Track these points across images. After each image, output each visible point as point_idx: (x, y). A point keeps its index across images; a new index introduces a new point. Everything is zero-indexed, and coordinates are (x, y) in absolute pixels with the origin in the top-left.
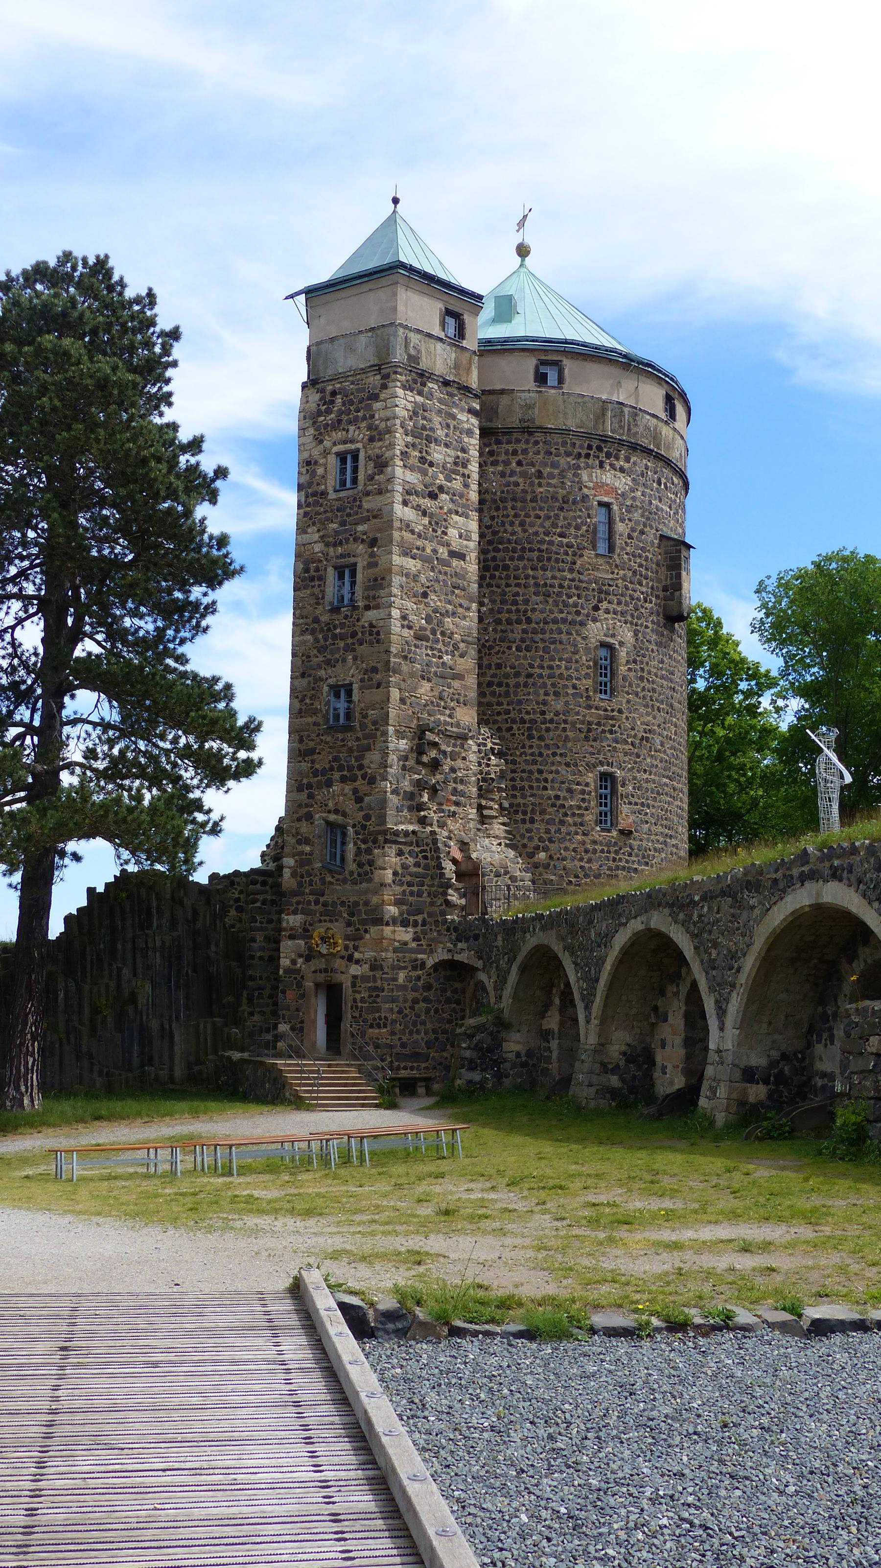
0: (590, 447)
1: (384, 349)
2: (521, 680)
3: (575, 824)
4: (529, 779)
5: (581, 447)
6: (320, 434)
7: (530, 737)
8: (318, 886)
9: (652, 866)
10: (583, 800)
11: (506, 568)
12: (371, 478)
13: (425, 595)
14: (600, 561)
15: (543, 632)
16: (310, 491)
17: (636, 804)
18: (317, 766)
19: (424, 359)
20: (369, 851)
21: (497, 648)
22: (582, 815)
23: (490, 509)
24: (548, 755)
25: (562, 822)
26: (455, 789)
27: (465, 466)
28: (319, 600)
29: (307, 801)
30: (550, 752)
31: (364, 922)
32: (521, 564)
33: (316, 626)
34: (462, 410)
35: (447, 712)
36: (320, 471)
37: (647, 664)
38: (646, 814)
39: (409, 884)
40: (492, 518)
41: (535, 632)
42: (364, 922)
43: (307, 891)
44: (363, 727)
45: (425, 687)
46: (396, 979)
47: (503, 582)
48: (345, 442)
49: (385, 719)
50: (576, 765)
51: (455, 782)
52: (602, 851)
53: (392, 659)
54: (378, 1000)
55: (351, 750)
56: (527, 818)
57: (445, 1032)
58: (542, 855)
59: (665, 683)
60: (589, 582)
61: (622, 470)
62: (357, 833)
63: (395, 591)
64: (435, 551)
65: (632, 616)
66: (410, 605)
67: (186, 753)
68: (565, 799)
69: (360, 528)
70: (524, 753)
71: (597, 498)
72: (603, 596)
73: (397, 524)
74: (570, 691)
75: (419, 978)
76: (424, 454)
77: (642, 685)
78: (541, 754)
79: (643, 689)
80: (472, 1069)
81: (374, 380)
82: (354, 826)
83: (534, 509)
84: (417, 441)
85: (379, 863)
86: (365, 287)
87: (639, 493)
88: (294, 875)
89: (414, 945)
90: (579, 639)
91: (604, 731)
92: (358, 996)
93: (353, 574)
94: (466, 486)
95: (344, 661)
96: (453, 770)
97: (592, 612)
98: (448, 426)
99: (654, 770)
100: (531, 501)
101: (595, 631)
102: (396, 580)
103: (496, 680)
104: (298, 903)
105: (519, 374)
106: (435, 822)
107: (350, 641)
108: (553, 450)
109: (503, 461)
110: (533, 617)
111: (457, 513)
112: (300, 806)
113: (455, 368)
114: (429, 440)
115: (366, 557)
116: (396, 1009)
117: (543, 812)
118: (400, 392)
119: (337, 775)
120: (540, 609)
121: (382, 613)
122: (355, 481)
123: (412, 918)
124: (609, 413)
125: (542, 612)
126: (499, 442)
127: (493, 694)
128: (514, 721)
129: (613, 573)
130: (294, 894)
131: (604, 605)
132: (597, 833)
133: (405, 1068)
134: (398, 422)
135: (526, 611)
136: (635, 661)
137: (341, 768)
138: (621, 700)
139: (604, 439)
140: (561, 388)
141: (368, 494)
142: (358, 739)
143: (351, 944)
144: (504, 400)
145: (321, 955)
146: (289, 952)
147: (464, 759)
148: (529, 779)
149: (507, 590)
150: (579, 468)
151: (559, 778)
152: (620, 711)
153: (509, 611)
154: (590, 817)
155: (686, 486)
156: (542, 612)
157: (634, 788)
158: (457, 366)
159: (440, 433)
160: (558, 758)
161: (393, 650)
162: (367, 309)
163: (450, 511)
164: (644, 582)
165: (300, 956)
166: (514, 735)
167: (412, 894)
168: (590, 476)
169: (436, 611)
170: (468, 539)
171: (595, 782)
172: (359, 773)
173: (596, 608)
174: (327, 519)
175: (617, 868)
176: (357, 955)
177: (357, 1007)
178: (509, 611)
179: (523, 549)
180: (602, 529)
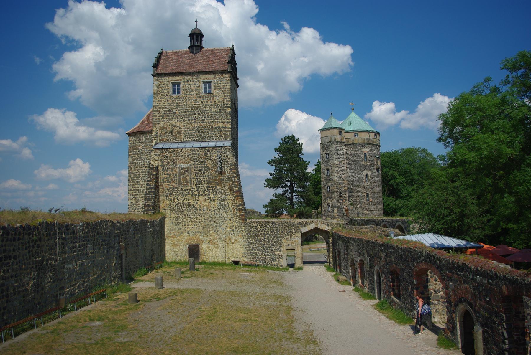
1: (331, 139)
139: (365, 144)
154: (365, 200)
162: (328, 133)
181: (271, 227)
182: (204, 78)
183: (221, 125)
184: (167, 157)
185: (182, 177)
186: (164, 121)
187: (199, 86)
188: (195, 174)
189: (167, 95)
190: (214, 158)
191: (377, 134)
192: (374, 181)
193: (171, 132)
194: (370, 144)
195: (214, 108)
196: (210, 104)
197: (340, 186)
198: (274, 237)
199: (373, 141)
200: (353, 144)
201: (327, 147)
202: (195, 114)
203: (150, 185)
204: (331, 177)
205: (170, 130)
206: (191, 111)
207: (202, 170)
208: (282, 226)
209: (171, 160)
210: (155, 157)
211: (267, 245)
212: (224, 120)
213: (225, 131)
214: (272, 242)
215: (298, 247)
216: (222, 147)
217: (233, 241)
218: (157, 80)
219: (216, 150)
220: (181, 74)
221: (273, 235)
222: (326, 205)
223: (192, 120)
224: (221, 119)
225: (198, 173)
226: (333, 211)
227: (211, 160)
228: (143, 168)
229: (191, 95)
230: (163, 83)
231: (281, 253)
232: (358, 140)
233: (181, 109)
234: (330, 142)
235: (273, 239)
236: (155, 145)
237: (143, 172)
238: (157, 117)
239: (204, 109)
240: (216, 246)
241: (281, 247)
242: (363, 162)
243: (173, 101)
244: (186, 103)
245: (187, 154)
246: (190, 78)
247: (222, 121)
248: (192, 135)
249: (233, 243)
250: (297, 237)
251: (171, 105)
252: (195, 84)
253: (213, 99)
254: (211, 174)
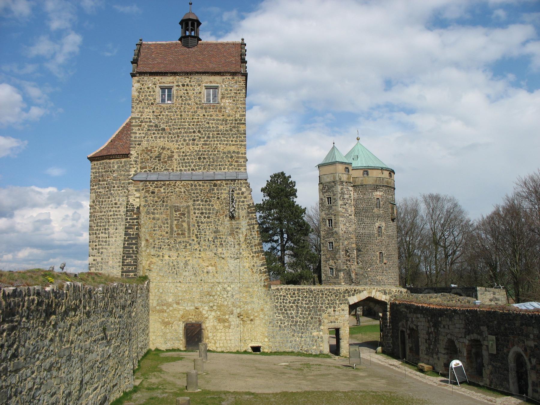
1: (334, 178)
81: (333, 184)
154: (378, 261)
159: (346, 192)
181: (306, 297)
182: (207, 80)
183: (233, 148)
184: (153, 193)
185: (175, 222)
186: (148, 141)
187: (200, 93)
188: (195, 218)
189: (152, 104)
190: (224, 196)
191: (392, 172)
192: (389, 236)
193: (159, 157)
194: (383, 186)
195: (222, 125)
196: (215, 118)
197: (346, 243)
198: (311, 311)
199: (387, 182)
200: (362, 185)
201: (329, 189)
202: (194, 132)
203: (130, 234)
204: (335, 229)
205: (157, 154)
206: (189, 128)
207: (206, 213)
208: (322, 294)
209: (159, 198)
210: (135, 193)
211: (300, 322)
212: (236, 141)
213: (238, 158)
214: (307, 318)
215: (344, 324)
216: (235, 180)
217: (252, 317)
218: (138, 82)
219: (227, 184)
220: (174, 74)
221: (309, 307)
222: (328, 268)
223: (190, 140)
224: (232, 141)
225: (200, 217)
226: (337, 277)
227: (218, 198)
228: (114, 209)
229: (189, 104)
230: (146, 87)
231: (321, 333)
232: (369, 180)
233: (173, 125)
234: (334, 182)
235: (309, 314)
236: (134, 175)
237: (114, 215)
238: (138, 135)
239: (207, 125)
240: (226, 324)
241: (320, 325)
242: (376, 210)
243: (161, 112)
244: (181, 115)
245: (183, 190)
246: (188, 80)
247: (234, 143)
248: (189, 163)
249: (252, 320)
250: (343, 310)
251: (158, 118)
252: (194, 90)
253: (220, 111)
254: (219, 220)
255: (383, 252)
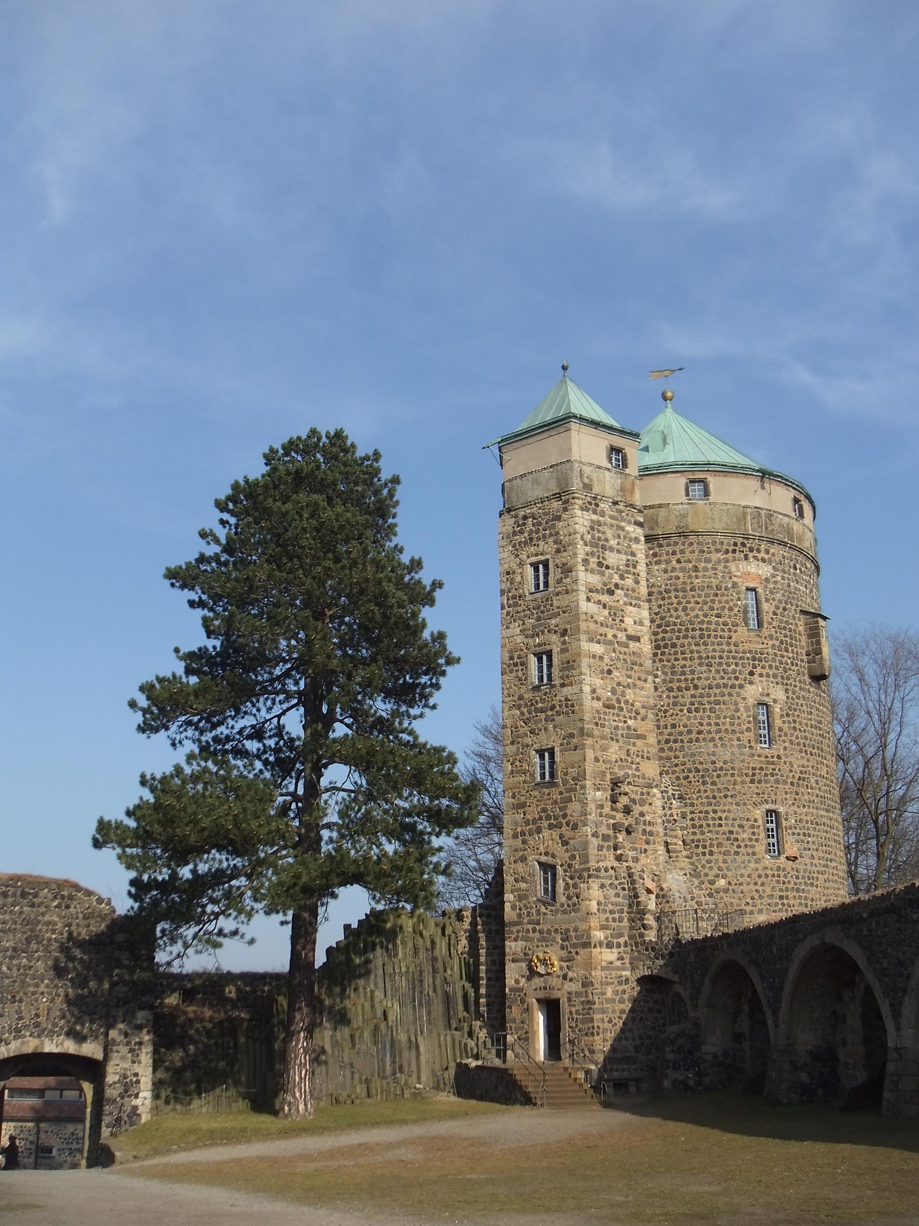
0: (735, 544)
2: (694, 736)
3: (748, 854)
4: (706, 818)
5: (729, 544)
6: (517, 550)
7: (704, 783)
8: (534, 917)
9: (817, 886)
10: (754, 833)
11: (674, 645)
12: (559, 581)
13: (609, 672)
14: (752, 634)
15: (709, 696)
16: (510, 595)
17: (799, 834)
18: (528, 817)
19: (596, 485)
20: (575, 886)
21: (672, 711)
22: (754, 846)
23: (657, 599)
24: (720, 797)
25: (737, 853)
26: (644, 830)
27: (635, 567)
28: (523, 680)
29: (522, 846)
30: (722, 795)
31: (575, 946)
32: (686, 641)
33: (521, 702)
34: (629, 523)
35: (634, 766)
36: (518, 579)
37: (798, 716)
38: (808, 843)
39: (611, 912)
40: (660, 606)
41: (702, 696)
42: (575, 946)
43: (525, 921)
44: (565, 782)
45: (614, 747)
46: (604, 994)
47: (673, 657)
48: (537, 555)
49: (582, 775)
50: (745, 804)
51: (645, 824)
52: (773, 875)
53: (586, 726)
54: (591, 1012)
55: (556, 802)
56: (707, 851)
57: (650, 1037)
58: (722, 882)
59: (815, 731)
60: (744, 652)
61: (763, 560)
62: (565, 871)
63: (584, 670)
64: (615, 636)
65: (782, 677)
66: (598, 682)
67: (421, 811)
68: (738, 833)
69: (553, 621)
70: (700, 796)
71: (745, 584)
72: (757, 662)
73: (583, 617)
74: (736, 743)
75: (624, 992)
76: (601, 560)
77: (796, 734)
78: (714, 797)
79: (797, 738)
80: (675, 1069)
81: (556, 505)
82: (562, 865)
83: (693, 596)
84: (595, 550)
85: (584, 895)
86: (546, 435)
87: (779, 578)
88: (513, 908)
89: (618, 963)
90: (739, 699)
91: (766, 775)
92: (573, 1009)
93: (550, 659)
94: (637, 582)
95: (546, 729)
96: (642, 814)
97: (748, 677)
98: (619, 536)
99: (811, 805)
100: (691, 590)
101: (752, 692)
102: (585, 662)
103: (672, 738)
104: (518, 932)
105: (672, 491)
106: (630, 859)
107: (550, 713)
108: (705, 549)
109: (665, 561)
110: (699, 684)
111: (631, 604)
112: (516, 850)
113: (621, 491)
114: (604, 547)
115: (560, 644)
116: (606, 1020)
117: (719, 845)
118: (578, 512)
119: (545, 824)
120: (705, 676)
121: (575, 689)
122: (546, 584)
123: (615, 941)
124: (749, 517)
125: (707, 679)
126: (660, 546)
127: (670, 749)
128: (690, 771)
129: (763, 643)
130: (515, 924)
131: (759, 670)
132: (768, 860)
133: (617, 1070)
134: (578, 536)
135: (693, 680)
136: (788, 715)
137: (548, 818)
138: (778, 748)
140: (708, 499)
141: (557, 594)
142: (561, 793)
143: (564, 964)
144: (663, 512)
145: (541, 975)
146: (513, 974)
147: (651, 804)
148: (706, 818)
149: (676, 663)
150: (727, 561)
151: (731, 815)
152: (779, 757)
153: (679, 681)
154: (760, 848)
155: (817, 568)
156: (707, 679)
157: (796, 821)
158: (622, 489)
159: (613, 543)
160: (729, 800)
161: (587, 717)
163: (625, 604)
164: (790, 649)
165: (523, 976)
166: (691, 782)
167: (614, 920)
168: (737, 567)
169: (619, 684)
170: (641, 624)
171: (762, 818)
172: (564, 821)
173: (752, 673)
174: (525, 616)
175: (787, 890)
176: (570, 974)
177: (573, 1019)
178: (679, 681)
179: (687, 630)
180: (752, 609)
197: (614, 751)
200: (683, 534)
255: (781, 809)
